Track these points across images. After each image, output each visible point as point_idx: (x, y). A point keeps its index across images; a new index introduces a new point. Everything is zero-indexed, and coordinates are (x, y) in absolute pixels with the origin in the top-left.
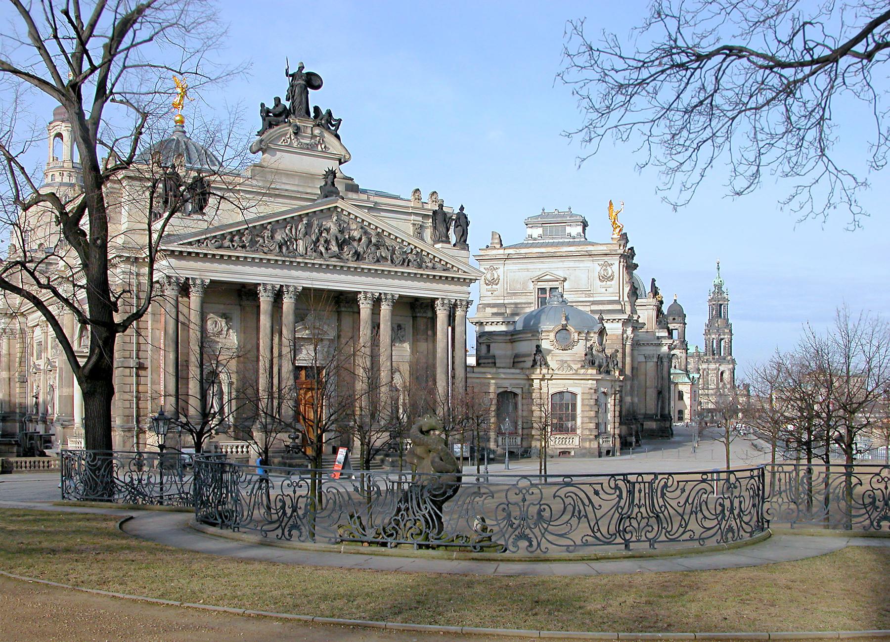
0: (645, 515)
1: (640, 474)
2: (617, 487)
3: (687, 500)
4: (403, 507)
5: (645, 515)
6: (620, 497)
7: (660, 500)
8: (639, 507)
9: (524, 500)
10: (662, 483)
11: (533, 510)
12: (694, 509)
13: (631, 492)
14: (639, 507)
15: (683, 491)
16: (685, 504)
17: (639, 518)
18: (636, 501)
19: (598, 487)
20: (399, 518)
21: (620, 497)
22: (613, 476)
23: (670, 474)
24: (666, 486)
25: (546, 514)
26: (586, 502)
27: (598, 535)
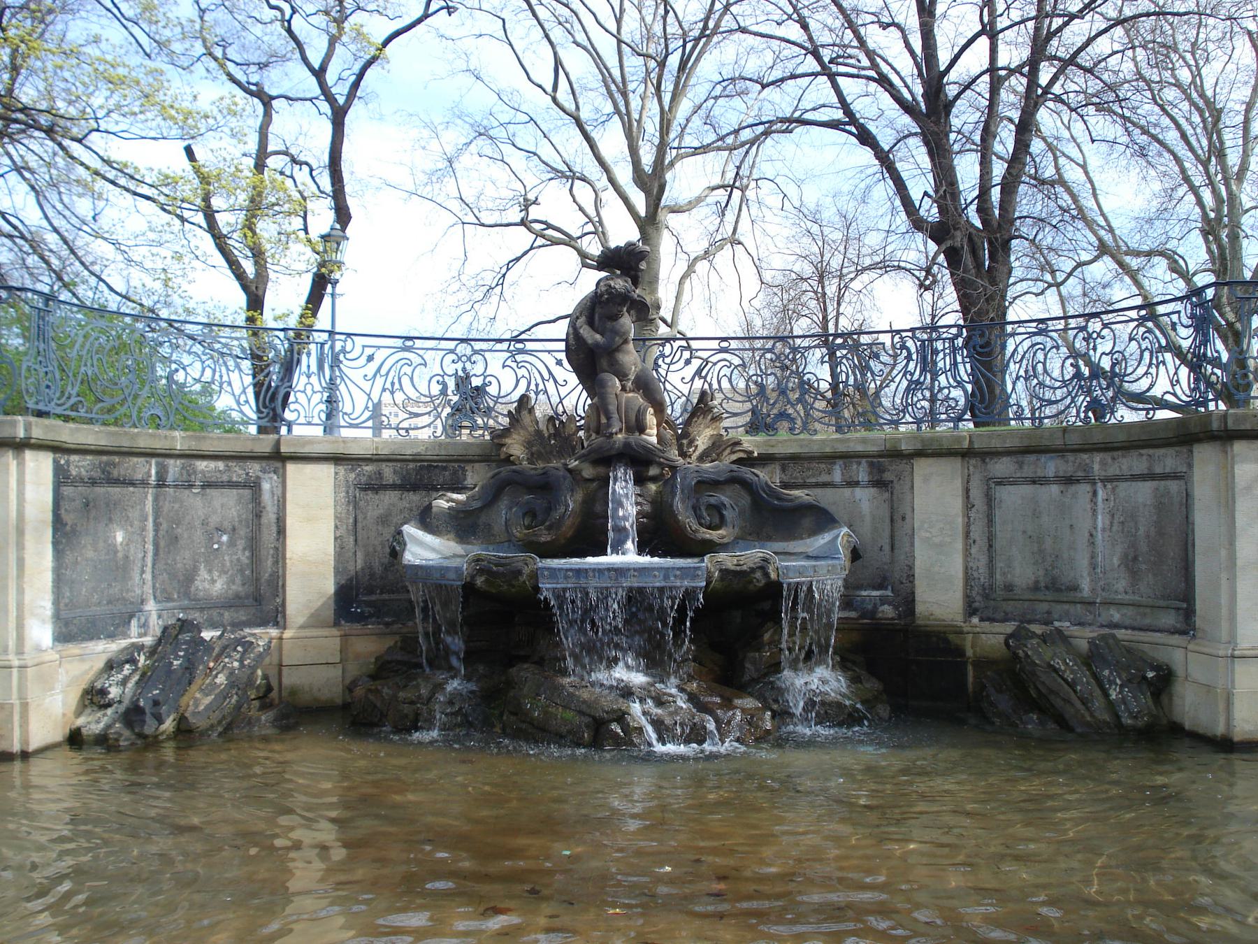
3: (379, 370)
8: (309, 377)
12: (388, 385)
14: (309, 377)
15: (370, 358)
16: (375, 376)
17: (309, 392)
23: (349, 335)
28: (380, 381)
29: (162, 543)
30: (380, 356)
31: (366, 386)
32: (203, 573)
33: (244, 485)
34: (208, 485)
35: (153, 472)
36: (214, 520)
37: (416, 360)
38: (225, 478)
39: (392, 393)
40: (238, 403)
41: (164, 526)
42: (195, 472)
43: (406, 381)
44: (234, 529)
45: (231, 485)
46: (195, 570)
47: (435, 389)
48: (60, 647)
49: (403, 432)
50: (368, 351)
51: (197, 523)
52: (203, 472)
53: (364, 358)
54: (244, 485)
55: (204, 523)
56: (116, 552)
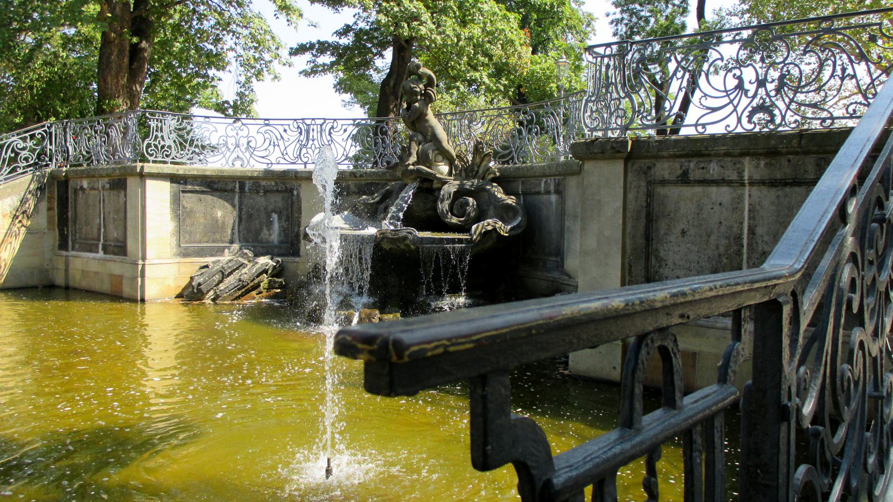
0: (317, 146)
1: (313, 119)
2: (299, 127)
4: (159, 135)
5: (317, 146)
6: (301, 133)
7: (329, 138)
9: (237, 134)
10: (330, 126)
11: (244, 141)
13: (308, 132)
15: (345, 131)
18: (311, 137)
19: (287, 127)
20: (157, 143)
21: (301, 133)
22: (295, 120)
23: (335, 120)
24: (332, 127)
25: (252, 144)
26: (279, 137)
27: (286, 157)
29: (244, 217)
31: (343, 144)
32: (265, 231)
34: (266, 192)
35: (237, 186)
36: (271, 207)
41: (245, 210)
42: (260, 186)
45: (277, 191)
46: (261, 229)
48: (179, 259)
50: (344, 127)
51: (262, 209)
53: (342, 131)
56: (217, 221)
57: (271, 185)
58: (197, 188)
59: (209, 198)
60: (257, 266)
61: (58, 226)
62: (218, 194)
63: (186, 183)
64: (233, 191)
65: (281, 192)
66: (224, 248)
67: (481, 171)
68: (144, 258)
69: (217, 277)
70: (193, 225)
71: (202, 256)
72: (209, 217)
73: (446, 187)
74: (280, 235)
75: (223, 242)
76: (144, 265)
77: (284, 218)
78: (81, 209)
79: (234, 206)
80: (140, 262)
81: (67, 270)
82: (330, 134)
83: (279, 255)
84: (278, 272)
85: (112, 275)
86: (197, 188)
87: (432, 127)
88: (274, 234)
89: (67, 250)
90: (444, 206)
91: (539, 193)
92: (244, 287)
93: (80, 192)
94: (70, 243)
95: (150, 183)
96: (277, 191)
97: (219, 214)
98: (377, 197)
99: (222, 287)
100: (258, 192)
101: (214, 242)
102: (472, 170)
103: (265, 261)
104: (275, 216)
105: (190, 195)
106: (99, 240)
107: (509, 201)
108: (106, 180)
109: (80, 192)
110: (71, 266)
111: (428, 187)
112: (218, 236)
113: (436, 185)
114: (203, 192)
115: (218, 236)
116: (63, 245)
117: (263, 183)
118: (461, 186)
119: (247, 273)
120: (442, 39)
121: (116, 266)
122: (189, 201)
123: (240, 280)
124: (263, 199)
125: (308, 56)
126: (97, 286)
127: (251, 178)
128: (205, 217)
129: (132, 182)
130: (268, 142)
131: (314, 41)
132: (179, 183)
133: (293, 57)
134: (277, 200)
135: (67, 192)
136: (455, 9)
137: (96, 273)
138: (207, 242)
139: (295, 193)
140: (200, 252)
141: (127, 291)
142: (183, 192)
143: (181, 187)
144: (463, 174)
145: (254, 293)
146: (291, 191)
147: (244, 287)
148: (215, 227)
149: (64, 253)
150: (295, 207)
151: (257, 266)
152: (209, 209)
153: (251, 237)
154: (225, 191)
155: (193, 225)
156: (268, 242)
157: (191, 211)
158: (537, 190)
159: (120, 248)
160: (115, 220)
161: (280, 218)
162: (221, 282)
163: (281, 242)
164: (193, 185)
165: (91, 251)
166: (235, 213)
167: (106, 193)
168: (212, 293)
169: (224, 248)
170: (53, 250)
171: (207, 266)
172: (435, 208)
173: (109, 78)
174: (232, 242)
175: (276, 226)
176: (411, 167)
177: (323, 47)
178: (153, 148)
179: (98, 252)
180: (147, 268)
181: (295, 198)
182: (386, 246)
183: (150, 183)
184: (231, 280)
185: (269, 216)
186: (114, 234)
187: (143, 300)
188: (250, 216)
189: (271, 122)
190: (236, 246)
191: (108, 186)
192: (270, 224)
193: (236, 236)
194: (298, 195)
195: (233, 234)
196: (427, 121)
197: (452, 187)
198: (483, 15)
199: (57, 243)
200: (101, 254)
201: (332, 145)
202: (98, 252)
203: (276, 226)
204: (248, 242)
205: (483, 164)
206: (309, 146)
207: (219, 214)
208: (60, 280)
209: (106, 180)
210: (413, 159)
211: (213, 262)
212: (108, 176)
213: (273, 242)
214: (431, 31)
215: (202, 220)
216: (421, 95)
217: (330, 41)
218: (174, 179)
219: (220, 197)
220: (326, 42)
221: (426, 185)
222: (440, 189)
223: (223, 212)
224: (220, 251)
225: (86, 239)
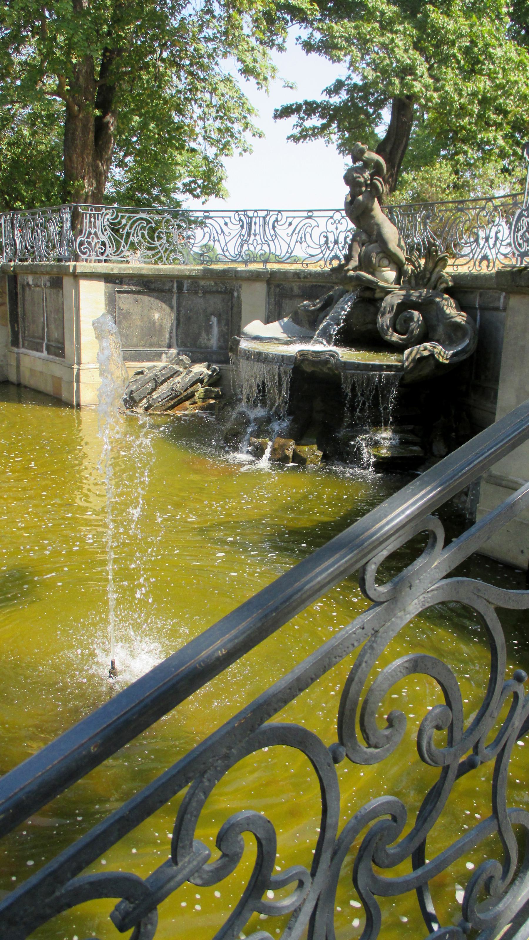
0: (259, 242)
1: (256, 211)
2: (240, 220)
3: (294, 230)
4: (93, 232)
5: (259, 242)
6: (242, 227)
7: (272, 232)
8: (255, 235)
10: (273, 218)
12: (299, 239)
13: (250, 225)
14: (255, 235)
15: (290, 224)
16: (292, 234)
17: (255, 244)
18: (253, 232)
19: (227, 220)
20: (90, 240)
21: (242, 227)
22: (237, 211)
23: (279, 211)
24: (276, 220)
26: (219, 231)
27: (227, 254)
28: (295, 236)
29: (182, 320)
30: (295, 222)
31: (288, 239)
32: (204, 335)
33: (225, 292)
35: (175, 286)
37: (314, 224)
38: (214, 289)
39: (301, 243)
40: (223, 251)
41: (183, 312)
42: (198, 286)
43: (308, 235)
44: (220, 315)
45: (217, 292)
46: (200, 334)
47: (323, 240)
49: (305, 266)
50: (290, 220)
51: (201, 311)
52: (203, 286)
53: (287, 224)
54: (225, 292)
55: (205, 311)
56: (154, 323)
57: (210, 285)
58: (133, 288)
59: (146, 299)
60: (191, 375)
61: (11, 321)
62: (155, 294)
63: (121, 283)
64: (170, 291)
65: (220, 292)
66: (162, 353)
67: (433, 279)
68: (79, 363)
69: (150, 386)
70: (129, 327)
71: (139, 361)
72: (146, 319)
73: (389, 298)
74: (219, 340)
75: (160, 346)
76: (79, 369)
77: (223, 322)
78: (28, 306)
79: (172, 308)
80: (76, 366)
81: (18, 367)
82: (274, 227)
83: (218, 362)
84: (216, 380)
85: (53, 377)
86: (133, 288)
87: (378, 225)
88: (213, 340)
89: (18, 347)
90: (385, 321)
91: (497, 309)
92: (177, 396)
93: (27, 289)
94: (21, 340)
95: (84, 284)
96: (217, 292)
97: (157, 316)
98: (318, 302)
99: (155, 395)
100: (196, 293)
101: (151, 346)
102: (423, 277)
103: (200, 369)
104: (214, 320)
105: (125, 295)
106: (43, 339)
107: (459, 319)
108: (47, 277)
109: (27, 289)
110: (22, 363)
111: (370, 298)
112: (155, 340)
113: (378, 295)
114: (139, 293)
115: (155, 340)
116: (15, 343)
117: (202, 283)
118: (407, 296)
119: (179, 382)
120: (440, 97)
121: (56, 369)
122: (126, 302)
123: (173, 390)
124: (201, 301)
125: (294, 119)
126: (41, 386)
127: (189, 277)
128: (142, 319)
129: (67, 282)
130: (207, 236)
131: (301, 101)
132: (114, 283)
133: (278, 121)
134: (216, 302)
135: (16, 287)
136: (459, 56)
137: (41, 373)
138: (144, 346)
139: (236, 294)
140: (137, 357)
141: (65, 395)
142: (119, 292)
143: (117, 287)
144: (413, 282)
145: (187, 403)
146: (231, 292)
147: (177, 396)
148: (152, 331)
149: (16, 350)
150: (235, 309)
151: (191, 375)
152: (146, 311)
153: (188, 341)
154: (163, 291)
155: (129, 327)
156: (207, 347)
157: (128, 312)
158: (496, 305)
159: (58, 350)
160: (55, 319)
161: (219, 322)
162: (154, 390)
163: (220, 348)
164: (129, 285)
165: (37, 350)
166: (173, 316)
167: (48, 291)
168: (145, 401)
169: (162, 353)
170: (6, 346)
171: (141, 373)
172: (375, 322)
173: (75, 156)
174: (170, 346)
175: (215, 330)
176: (351, 273)
177: (311, 108)
178: (86, 245)
179: (42, 351)
180: (82, 373)
181: (235, 300)
182: (308, 369)
183: (84, 284)
184: (164, 389)
185: (209, 320)
186: (56, 335)
187: (78, 405)
188: (189, 319)
189: (212, 214)
190: (174, 351)
191: (48, 284)
192: (208, 328)
193: (174, 341)
194: (239, 297)
195: (171, 338)
196: (373, 217)
197: (395, 298)
198: (493, 63)
199: (10, 339)
200: (45, 354)
201: (276, 241)
202: (42, 352)
203: (215, 330)
204: (185, 346)
205: (437, 270)
206: (251, 242)
207: (157, 316)
208: (13, 377)
209: (47, 277)
210: (354, 263)
211: (149, 369)
212: (47, 273)
213: (212, 347)
214: (426, 87)
215: (139, 323)
216: (367, 186)
217: (319, 101)
218: (108, 278)
219: (157, 298)
220: (314, 102)
221: (367, 294)
222: (382, 299)
223: (161, 314)
224: (157, 356)
225: (33, 337)
